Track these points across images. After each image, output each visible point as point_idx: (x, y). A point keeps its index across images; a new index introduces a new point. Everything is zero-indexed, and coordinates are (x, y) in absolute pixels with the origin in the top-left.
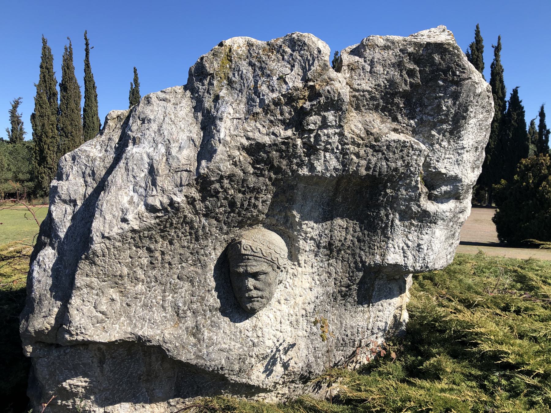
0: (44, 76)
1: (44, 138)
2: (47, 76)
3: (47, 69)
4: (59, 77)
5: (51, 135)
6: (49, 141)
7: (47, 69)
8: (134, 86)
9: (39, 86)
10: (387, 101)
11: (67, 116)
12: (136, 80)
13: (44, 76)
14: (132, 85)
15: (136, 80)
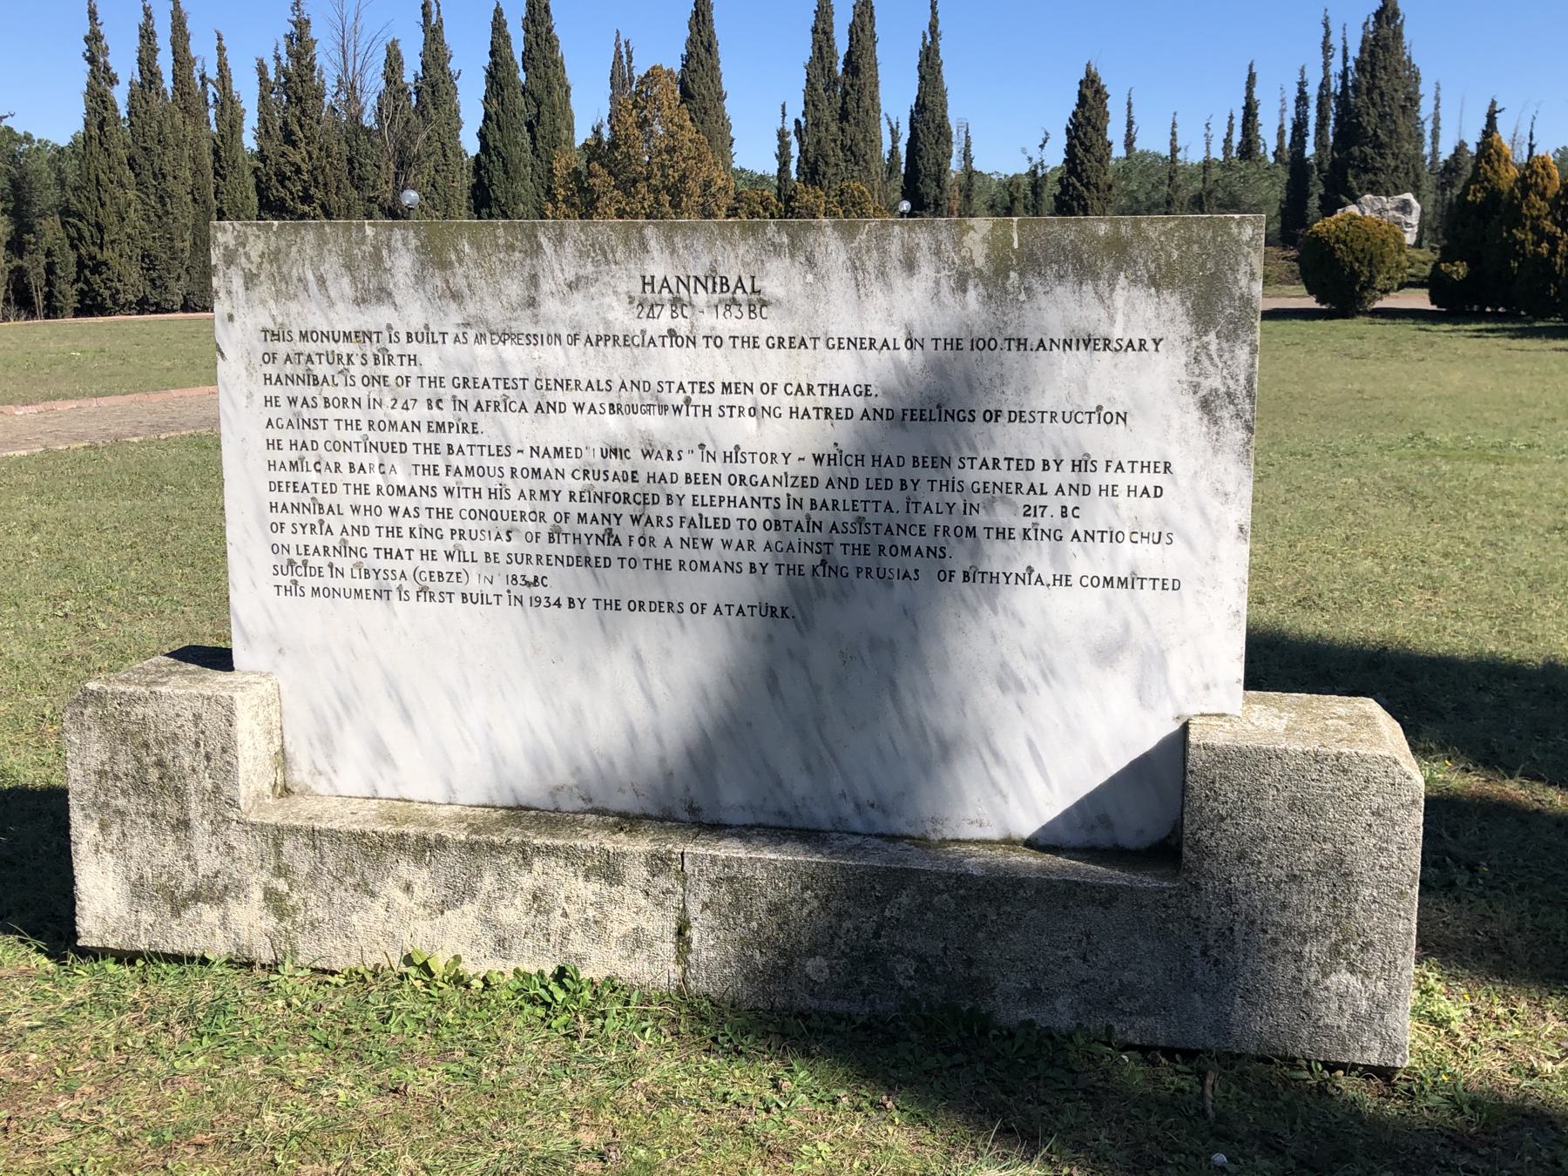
0: (820, 48)
1: (822, 167)
2: (825, 49)
3: (825, 33)
4: (842, 45)
5: (832, 160)
6: (831, 171)
7: (825, 33)
8: (929, 39)
9: (809, 67)
10: (1397, 209)
11: (857, 125)
12: (933, 27)
13: (820, 48)
14: (925, 38)
15: (933, 27)
